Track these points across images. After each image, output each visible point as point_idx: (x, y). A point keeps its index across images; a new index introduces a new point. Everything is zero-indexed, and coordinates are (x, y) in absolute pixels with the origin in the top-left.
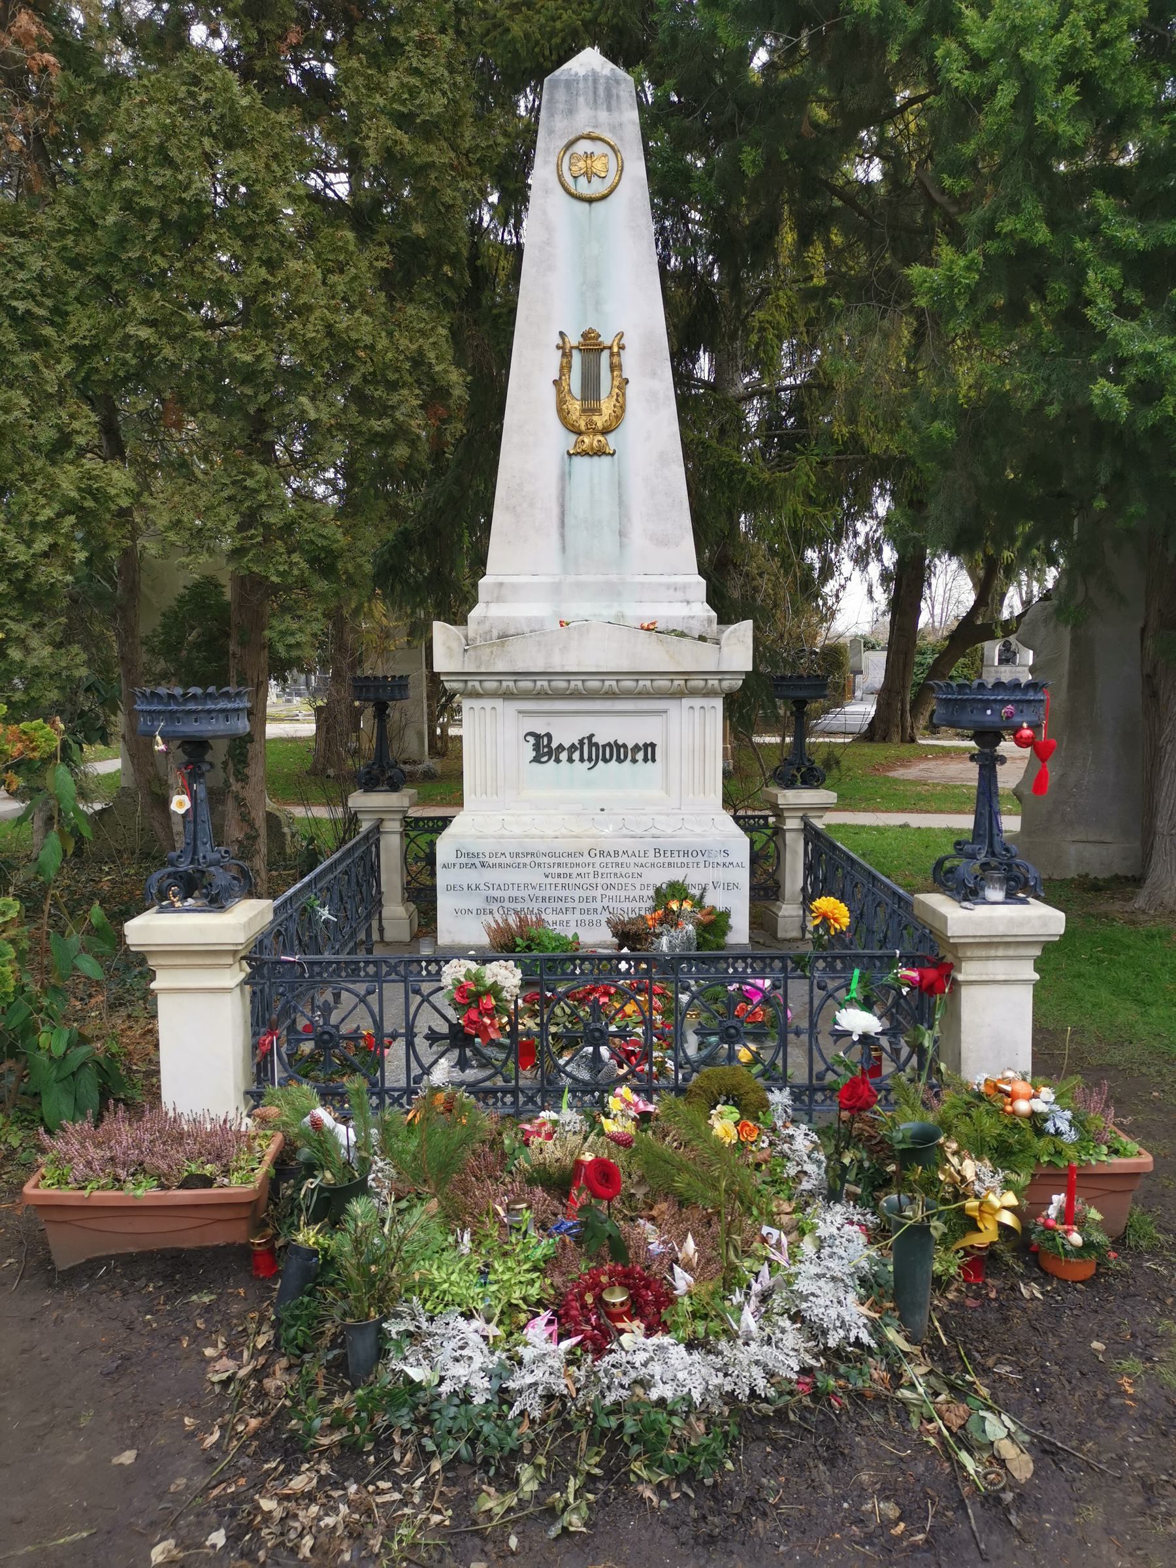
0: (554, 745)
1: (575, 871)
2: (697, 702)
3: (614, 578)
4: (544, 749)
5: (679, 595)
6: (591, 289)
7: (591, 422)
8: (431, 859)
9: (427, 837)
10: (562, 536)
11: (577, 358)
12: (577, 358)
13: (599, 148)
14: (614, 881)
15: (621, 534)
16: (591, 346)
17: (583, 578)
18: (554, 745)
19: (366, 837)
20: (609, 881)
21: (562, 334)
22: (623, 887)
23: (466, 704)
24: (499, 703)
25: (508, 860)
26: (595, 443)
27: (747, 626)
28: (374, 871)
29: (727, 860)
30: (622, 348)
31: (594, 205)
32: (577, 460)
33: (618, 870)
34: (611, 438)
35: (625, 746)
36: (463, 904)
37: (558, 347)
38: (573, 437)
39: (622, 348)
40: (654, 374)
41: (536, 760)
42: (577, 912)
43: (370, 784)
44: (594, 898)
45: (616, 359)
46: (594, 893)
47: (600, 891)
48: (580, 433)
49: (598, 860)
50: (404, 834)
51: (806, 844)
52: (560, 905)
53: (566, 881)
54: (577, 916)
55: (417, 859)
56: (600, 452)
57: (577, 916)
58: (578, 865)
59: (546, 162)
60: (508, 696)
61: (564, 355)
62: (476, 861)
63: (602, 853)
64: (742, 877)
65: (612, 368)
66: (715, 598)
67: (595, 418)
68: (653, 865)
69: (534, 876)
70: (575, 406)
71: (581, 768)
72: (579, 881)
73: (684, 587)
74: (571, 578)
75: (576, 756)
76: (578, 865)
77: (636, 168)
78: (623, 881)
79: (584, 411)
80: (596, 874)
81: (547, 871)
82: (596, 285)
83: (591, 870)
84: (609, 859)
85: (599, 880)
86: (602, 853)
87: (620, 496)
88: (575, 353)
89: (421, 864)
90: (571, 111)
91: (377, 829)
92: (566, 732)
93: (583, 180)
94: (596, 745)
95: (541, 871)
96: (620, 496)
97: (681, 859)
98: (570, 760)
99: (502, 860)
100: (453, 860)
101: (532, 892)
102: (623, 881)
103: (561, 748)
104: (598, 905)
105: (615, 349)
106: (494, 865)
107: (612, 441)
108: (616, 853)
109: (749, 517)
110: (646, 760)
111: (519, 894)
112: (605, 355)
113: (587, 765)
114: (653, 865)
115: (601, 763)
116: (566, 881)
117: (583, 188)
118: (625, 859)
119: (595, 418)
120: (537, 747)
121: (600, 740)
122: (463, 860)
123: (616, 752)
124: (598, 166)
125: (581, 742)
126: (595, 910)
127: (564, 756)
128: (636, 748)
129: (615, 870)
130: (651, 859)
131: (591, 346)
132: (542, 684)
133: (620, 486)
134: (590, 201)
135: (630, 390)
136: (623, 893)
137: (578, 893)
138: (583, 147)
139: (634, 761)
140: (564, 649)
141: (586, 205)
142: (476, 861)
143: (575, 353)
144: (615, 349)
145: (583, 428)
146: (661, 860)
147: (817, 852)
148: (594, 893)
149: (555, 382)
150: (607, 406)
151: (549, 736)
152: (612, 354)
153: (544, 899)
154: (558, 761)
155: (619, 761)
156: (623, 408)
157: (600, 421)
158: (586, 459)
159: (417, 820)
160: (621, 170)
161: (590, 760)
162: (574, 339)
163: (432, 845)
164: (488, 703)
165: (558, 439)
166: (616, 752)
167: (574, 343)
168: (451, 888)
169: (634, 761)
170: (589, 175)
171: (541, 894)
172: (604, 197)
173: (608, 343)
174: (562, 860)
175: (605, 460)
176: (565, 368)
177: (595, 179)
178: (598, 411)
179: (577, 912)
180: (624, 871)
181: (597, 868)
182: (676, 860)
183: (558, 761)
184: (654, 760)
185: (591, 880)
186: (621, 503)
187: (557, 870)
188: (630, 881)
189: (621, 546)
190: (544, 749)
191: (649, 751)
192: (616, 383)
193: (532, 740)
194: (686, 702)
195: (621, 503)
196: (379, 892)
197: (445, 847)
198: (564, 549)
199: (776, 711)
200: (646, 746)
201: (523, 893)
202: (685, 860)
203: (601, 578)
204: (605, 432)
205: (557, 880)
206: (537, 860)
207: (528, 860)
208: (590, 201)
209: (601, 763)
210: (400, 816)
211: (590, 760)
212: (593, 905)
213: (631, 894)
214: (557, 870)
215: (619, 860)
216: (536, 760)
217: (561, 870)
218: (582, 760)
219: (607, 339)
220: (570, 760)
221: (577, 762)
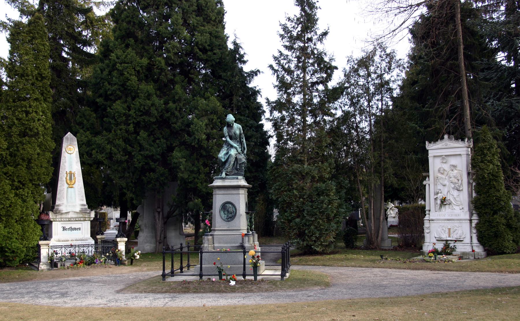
4: (64, 229)
6: (71, 165)
16: (71, 173)
23: (53, 222)
24: (58, 222)
56: (72, 187)
70: (69, 181)
92: (67, 227)
107: (74, 186)
117: (69, 152)
123: (75, 229)
132: (65, 219)
133: (75, 192)
150: (73, 181)
162: (68, 172)
164: (56, 222)
165: (66, 186)
166: (75, 229)
190: (64, 229)
191: (79, 229)
194: (85, 222)
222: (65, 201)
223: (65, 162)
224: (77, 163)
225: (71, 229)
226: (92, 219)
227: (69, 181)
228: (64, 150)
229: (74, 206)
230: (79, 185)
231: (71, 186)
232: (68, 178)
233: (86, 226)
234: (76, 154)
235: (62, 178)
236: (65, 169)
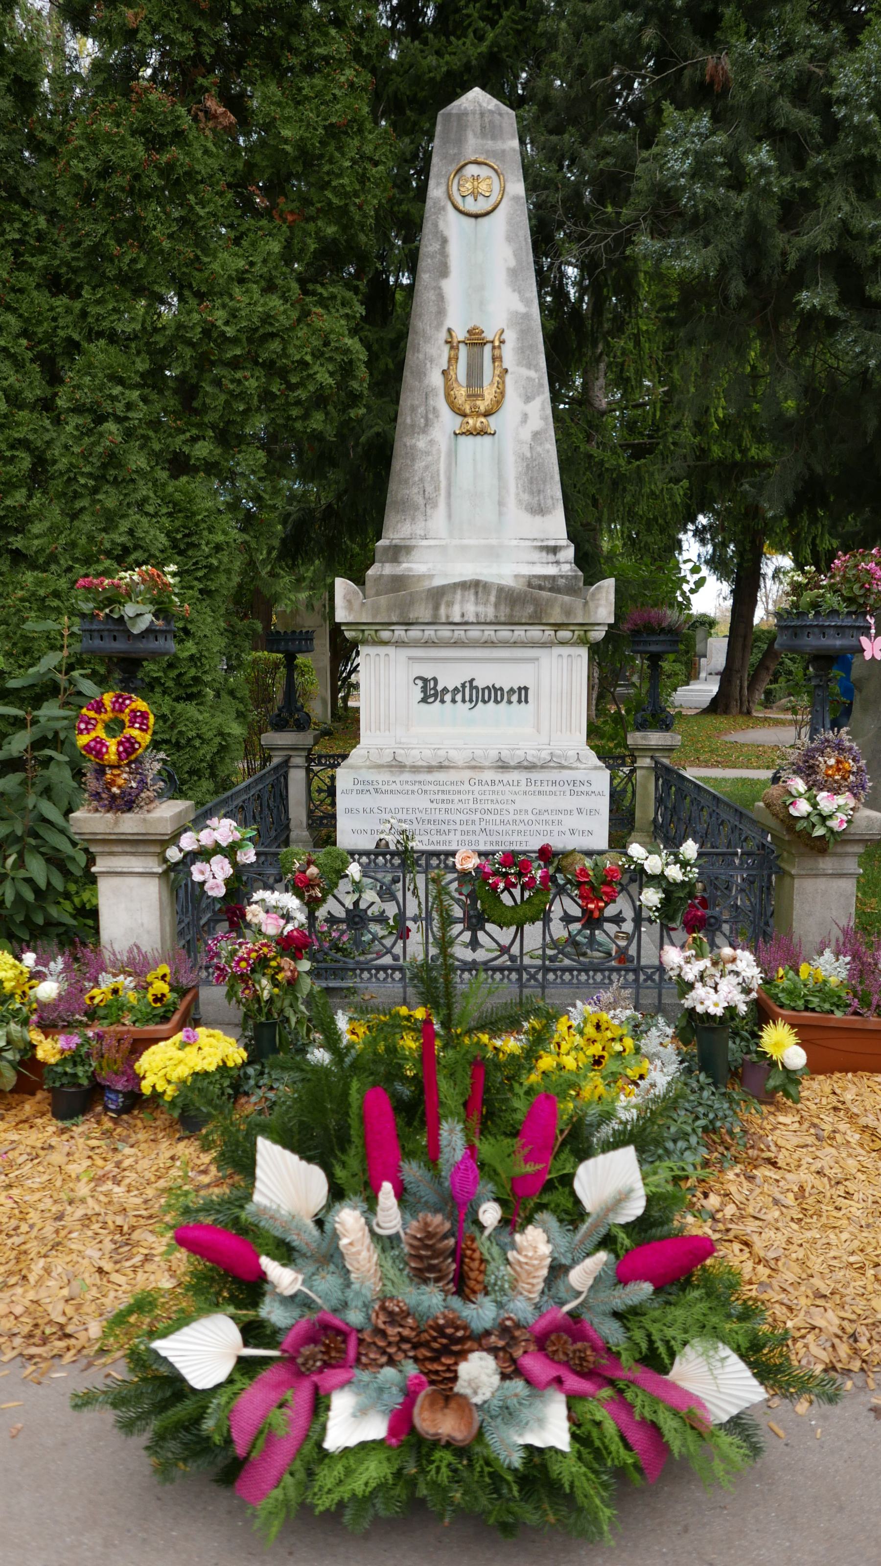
0: (439, 688)
1: (456, 797)
2: (565, 651)
3: (494, 542)
4: (431, 692)
5: (551, 558)
6: (477, 291)
7: (475, 406)
8: (331, 791)
9: (330, 772)
10: (449, 505)
11: (463, 351)
12: (463, 351)
13: (484, 172)
14: (490, 806)
15: (501, 503)
16: (476, 340)
17: (466, 542)
18: (439, 688)
19: (276, 768)
20: (486, 806)
21: (449, 331)
22: (499, 812)
25: (398, 787)
26: (478, 425)
27: (609, 584)
28: (283, 799)
29: (592, 788)
30: (502, 342)
31: (480, 220)
32: (463, 439)
33: (494, 797)
34: (492, 419)
35: (501, 689)
36: (358, 826)
37: (447, 342)
38: (459, 419)
39: (502, 342)
40: (529, 366)
41: (424, 700)
42: (458, 833)
43: (280, 725)
44: (473, 822)
45: (497, 352)
46: (473, 817)
47: (479, 815)
48: (465, 415)
49: (477, 788)
50: (308, 770)
51: (657, 780)
52: (445, 827)
53: (449, 806)
54: (458, 837)
55: (320, 791)
56: (482, 432)
57: (458, 837)
58: (459, 792)
59: (438, 184)
60: (400, 644)
61: (452, 348)
62: (371, 788)
63: (480, 782)
64: (603, 804)
65: (494, 359)
66: (581, 560)
67: (478, 403)
68: (525, 793)
69: (422, 802)
70: (461, 392)
71: (462, 708)
72: (460, 806)
73: (554, 550)
74: (456, 542)
75: (459, 697)
76: (459, 792)
77: (517, 187)
78: (498, 806)
79: (469, 396)
80: (475, 801)
81: (433, 797)
82: (481, 288)
83: (471, 797)
84: (486, 788)
85: (479, 806)
86: (480, 782)
87: (500, 471)
88: (461, 346)
89: (323, 795)
90: (460, 141)
91: (286, 764)
92: (450, 677)
93: (470, 199)
94: (477, 688)
95: (428, 797)
96: (500, 471)
97: (550, 788)
98: (454, 701)
99: (393, 787)
100: (350, 786)
101: (419, 815)
102: (498, 806)
103: (445, 690)
104: (477, 828)
105: (497, 343)
106: (386, 792)
107: (493, 423)
108: (493, 782)
109: (610, 493)
110: (520, 701)
111: (408, 817)
112: (488, 349)
113: (468, 705)
114: (525, 793)
115: (480, 704)
116: (449, 806)
117: (471, 205)
118: (500, 787)
119: (478, 403)
120: (424, 689)
121: (480, 683)
122: (359, 787)
124: (483, 187)
125: (463, 686)
126: (474, 832)
127: (448, 697)
128: (512, 690)
129: (494, 797)
130: (523, 787)
131: (476, 340)
133: (499, 462)
134: (476, 216)
135: (508, 378)
136: (498, 818)
137: (458, 817)
138: (472, 170)
139: (510, 702)
140: (450, 604)
141: (473, 220)
142: (371, 788)
143: (461, 346)
144: (497, 343)
145: (468, 411)
146: (532, 788)
147: (667, 785)
148: (473, 817)
149: (444, 372)
150: (489, 393)
151: (435, 680)
152: (494, 348)
153: (429, 821)
154: (443, 701)
155: (497, 702)
156: (503, 394)
157: (483, 406)
158: (470, 437)
159: (320, 757)
160: (503, 191)
161: (471, 701)
162: (460, 334)
163: (333, 778)
164: (382, 650)
165: (447, 421)
167: (461, 338)
168: (349, 811)
169: (510, 702)
170: (475, 195)
171: (426, 817)
172: (487, 214)
173: (490, 338)
174: (445, 788)
175: (487, 439)
176: (453, 360)
177: (480, 198)
178: (482, 396)
179: (458, 833)
180: (500, 798)
181: (476, 795)
182: (545, 788)
183: (443, 701)
184: (526, 702)
185: (471, 805)
186: (501, 477)
187: (441, 796)
188: (505, 806)
189: (501, 514)
190: (431, 692)
191: (522, 694)
192: (497, 372)
193: (420, 683)
194: (557, 650)
195: (501, 477)
196: (288, 819)
197: (344, 777)
198: (450, 516)
199: (633, 666)
200: (520, 689)
201: (412, 817)
202: (553, 789)
203: (483, 542)
204: (487, 414)
205: (440, 806)
206: (424, 788)
207: (416, 787)
208: (476, 216)
209: (480, 704)
210: (305, 753)
211: (471, 701)
212: (471, 828)
213: (506, 818)
214: (441, 796)
215: (495, 788)
216: (424, 700)
217: (445, 797)
218: (464, 701)
219: (489, 335)
220: (454, 701)
221: (459, 703)
222: (438, 521)
223: (443, 271)
224: (514, 273)
225: (475, 694)
226: (598, 634)
227: (461, 392)
228: (435, 191)
229: (493, 553)
230: (525, 417)
231: (476, 419)
232: (461, 370)
233: (562, 680)
234: (511, 222)
235: (421, 374)
236: (441, 312)
